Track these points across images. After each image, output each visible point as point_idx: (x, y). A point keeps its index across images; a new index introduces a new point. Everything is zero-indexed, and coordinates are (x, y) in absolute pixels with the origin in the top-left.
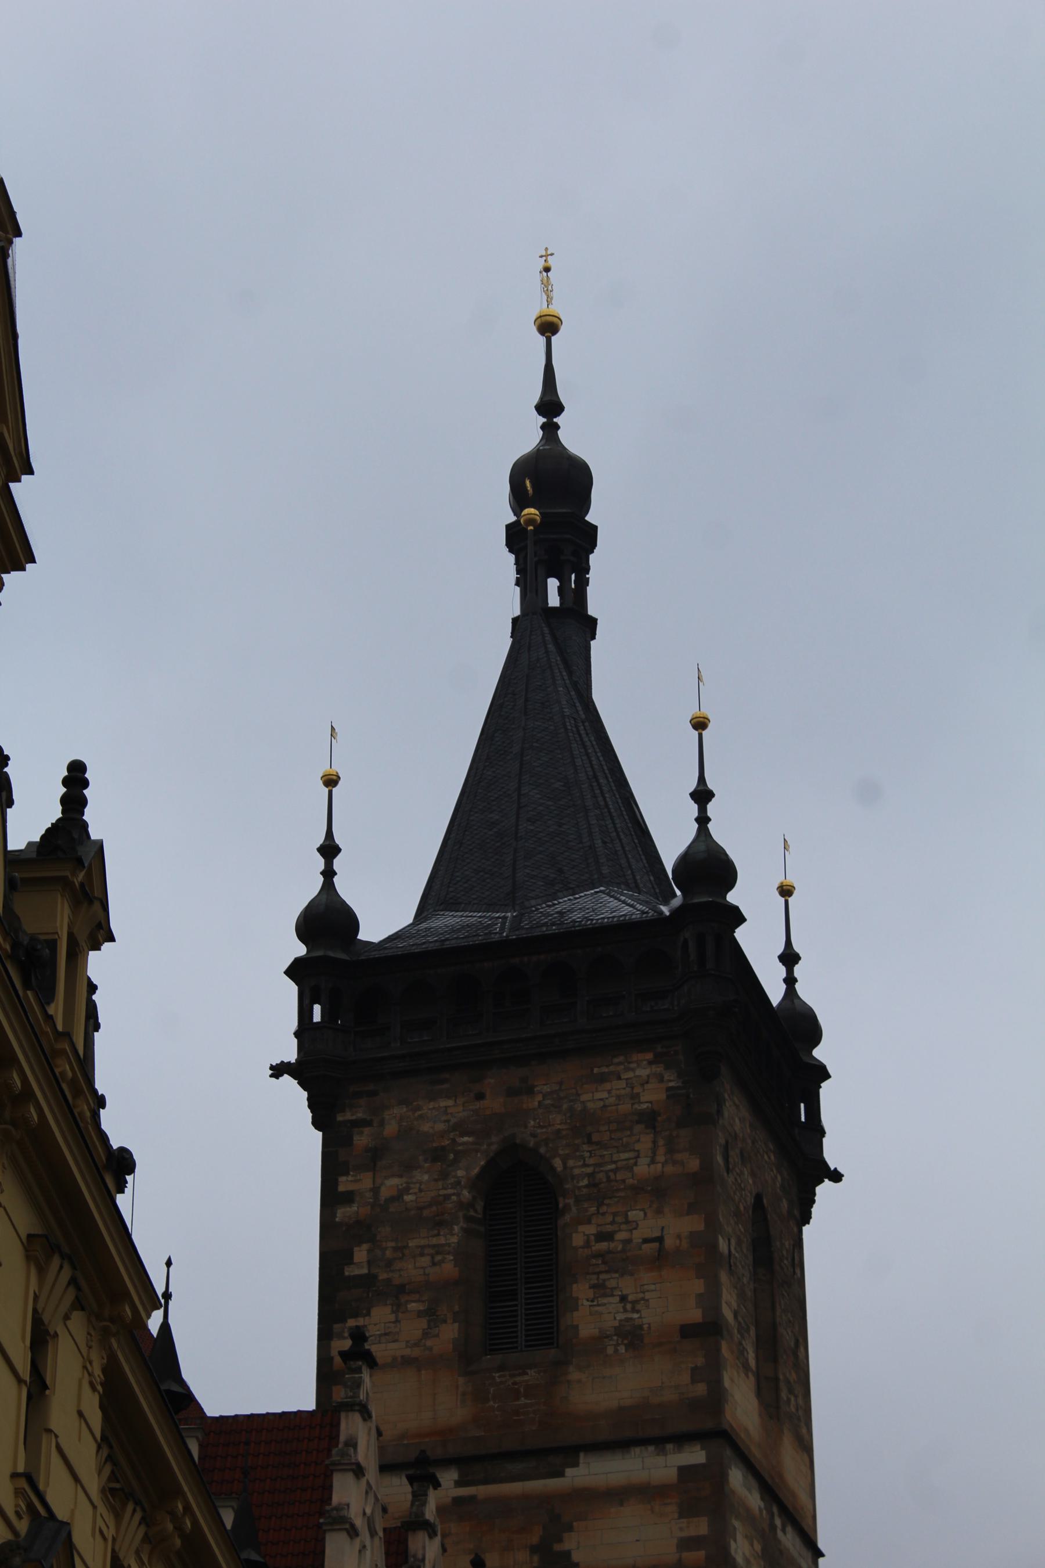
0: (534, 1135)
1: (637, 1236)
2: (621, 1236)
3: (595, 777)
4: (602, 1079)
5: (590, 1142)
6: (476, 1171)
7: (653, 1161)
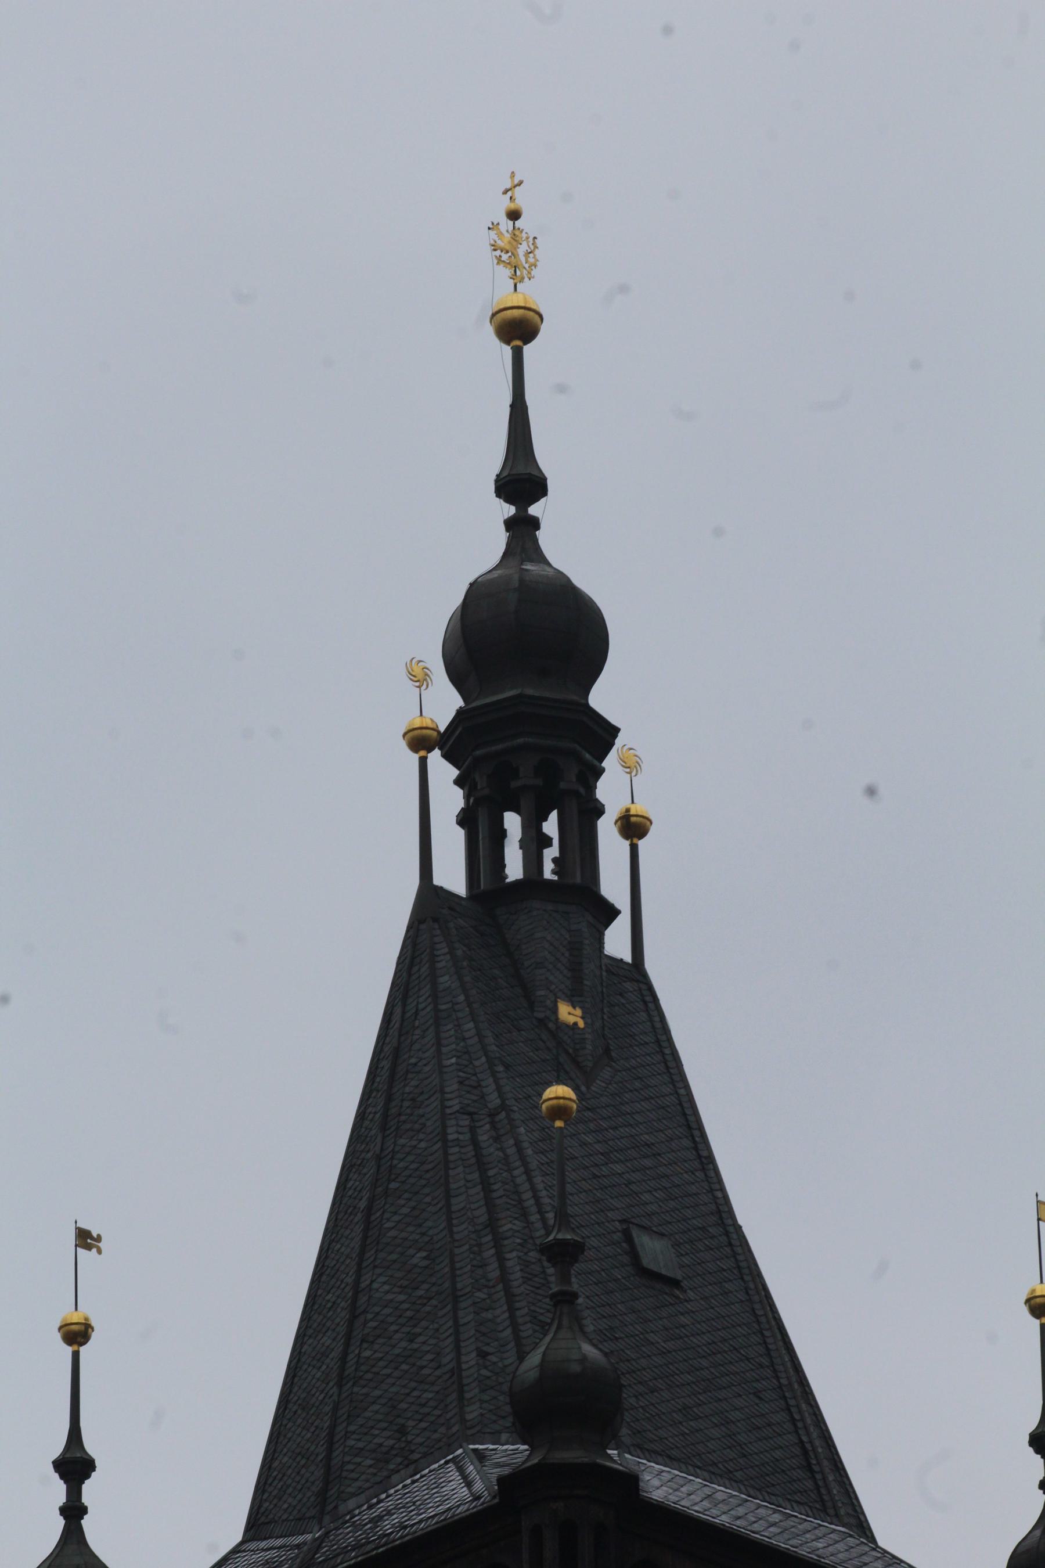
3: (492, 1224)
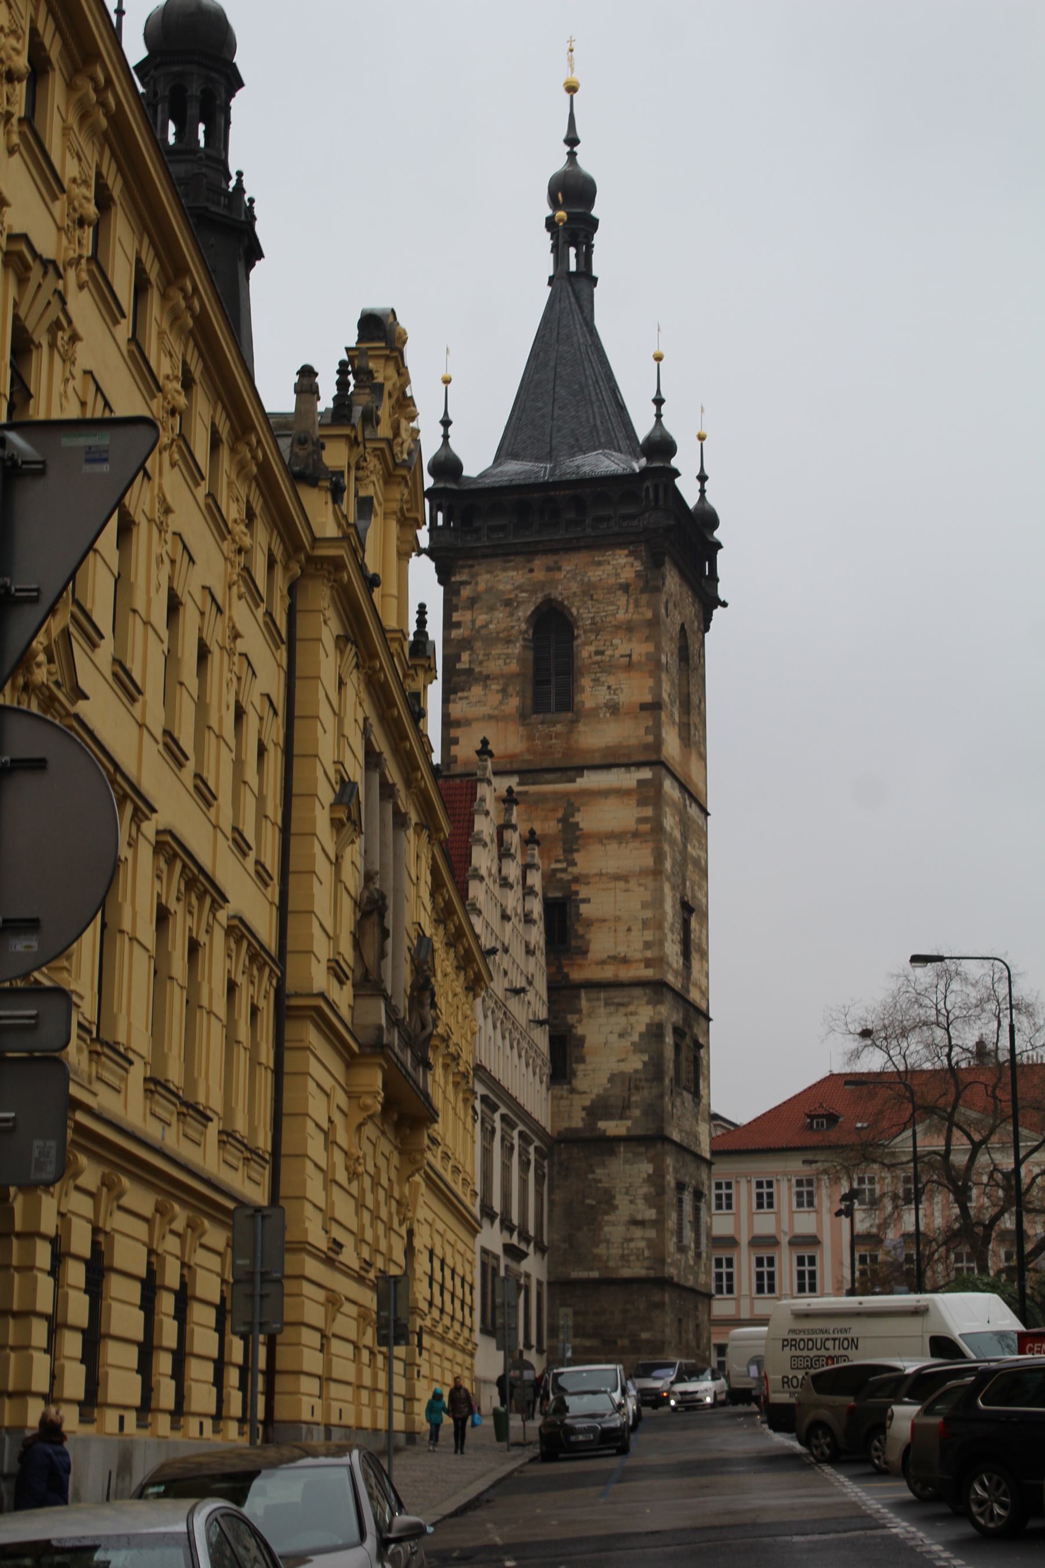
0: (561, 594)
1: (617, 653)
2: (608, 653)
3: (597, 381)
4: (600, 564)
5: (592, 599)
6: (529, 613)
7: (627, 611)
